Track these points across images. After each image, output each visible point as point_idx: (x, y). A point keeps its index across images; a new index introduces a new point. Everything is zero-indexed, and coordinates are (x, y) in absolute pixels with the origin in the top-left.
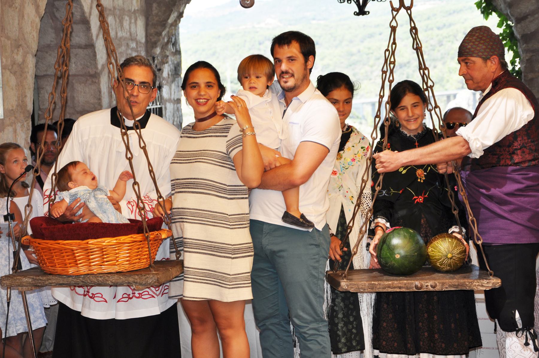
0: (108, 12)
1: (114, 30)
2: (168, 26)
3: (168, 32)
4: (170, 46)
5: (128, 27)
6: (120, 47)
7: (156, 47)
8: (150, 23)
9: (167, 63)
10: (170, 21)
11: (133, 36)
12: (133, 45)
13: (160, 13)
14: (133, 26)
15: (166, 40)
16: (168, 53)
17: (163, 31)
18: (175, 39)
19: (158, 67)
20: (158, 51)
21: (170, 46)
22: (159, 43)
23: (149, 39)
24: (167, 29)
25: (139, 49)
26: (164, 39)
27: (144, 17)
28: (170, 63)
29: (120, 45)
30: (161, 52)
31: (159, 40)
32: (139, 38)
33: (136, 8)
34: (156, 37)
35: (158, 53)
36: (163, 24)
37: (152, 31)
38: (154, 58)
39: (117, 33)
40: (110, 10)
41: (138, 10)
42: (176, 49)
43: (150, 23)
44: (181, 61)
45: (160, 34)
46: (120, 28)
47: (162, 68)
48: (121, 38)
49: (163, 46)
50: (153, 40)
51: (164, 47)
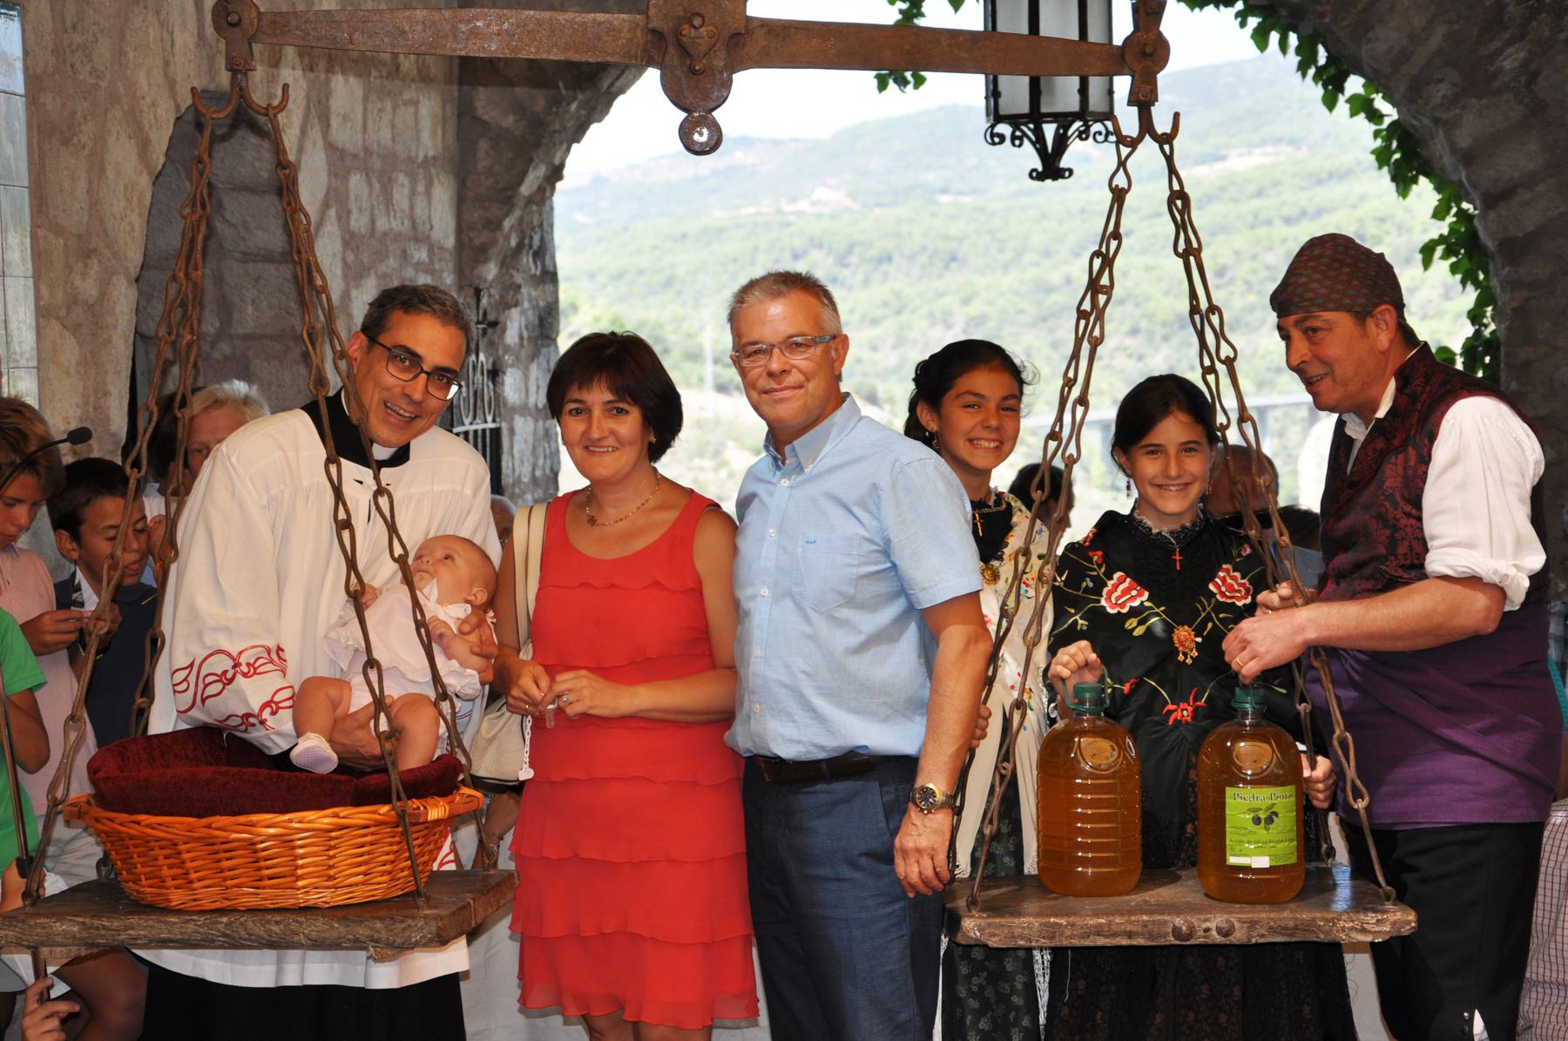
0: (348, 162)
1: (367, 214)
2: (521, 204)
3: (521, 219)
4: (527, 260)
5: (405, 205)
6: (382, 261)
7: (486, 261)
8: (471, 194)
9: (516, 305)
10: (526, 189)
11: (420, 228)
12: (421, 254)
13: (497, 168)
14: (420, 203)
15: (513, 242)
16: (519, 278)
17: (506, 216)
18: (542, 239)
19: (491, 317)
20: (491, 271)
21: (527, 260)
22: (494, 250)
23: (465, 240)
24: (517, 213)
25: (437, 266)
26: (507, 238)
27: (451, 178)
28: (526, 305)
29: (381, 256)
30: (499, 276)
31: (494, 243)
32: (436, 235)
33: (431, 154)
34: (486, 233)
35: (490, 277)
36: (506, 196)
37: (476, 216)
38: (478, 293)
39: (373, 222)
40: (356, 156)
41: (434, 158)
42: (543, 266)
43: (471, 194)
44: (556, 301)
45: (496, 225)
46: (382, 207)
47: (502, 318)
48: (385, 234)
49: (505, 258)
50: (478, 241)
51: (509, 261)
